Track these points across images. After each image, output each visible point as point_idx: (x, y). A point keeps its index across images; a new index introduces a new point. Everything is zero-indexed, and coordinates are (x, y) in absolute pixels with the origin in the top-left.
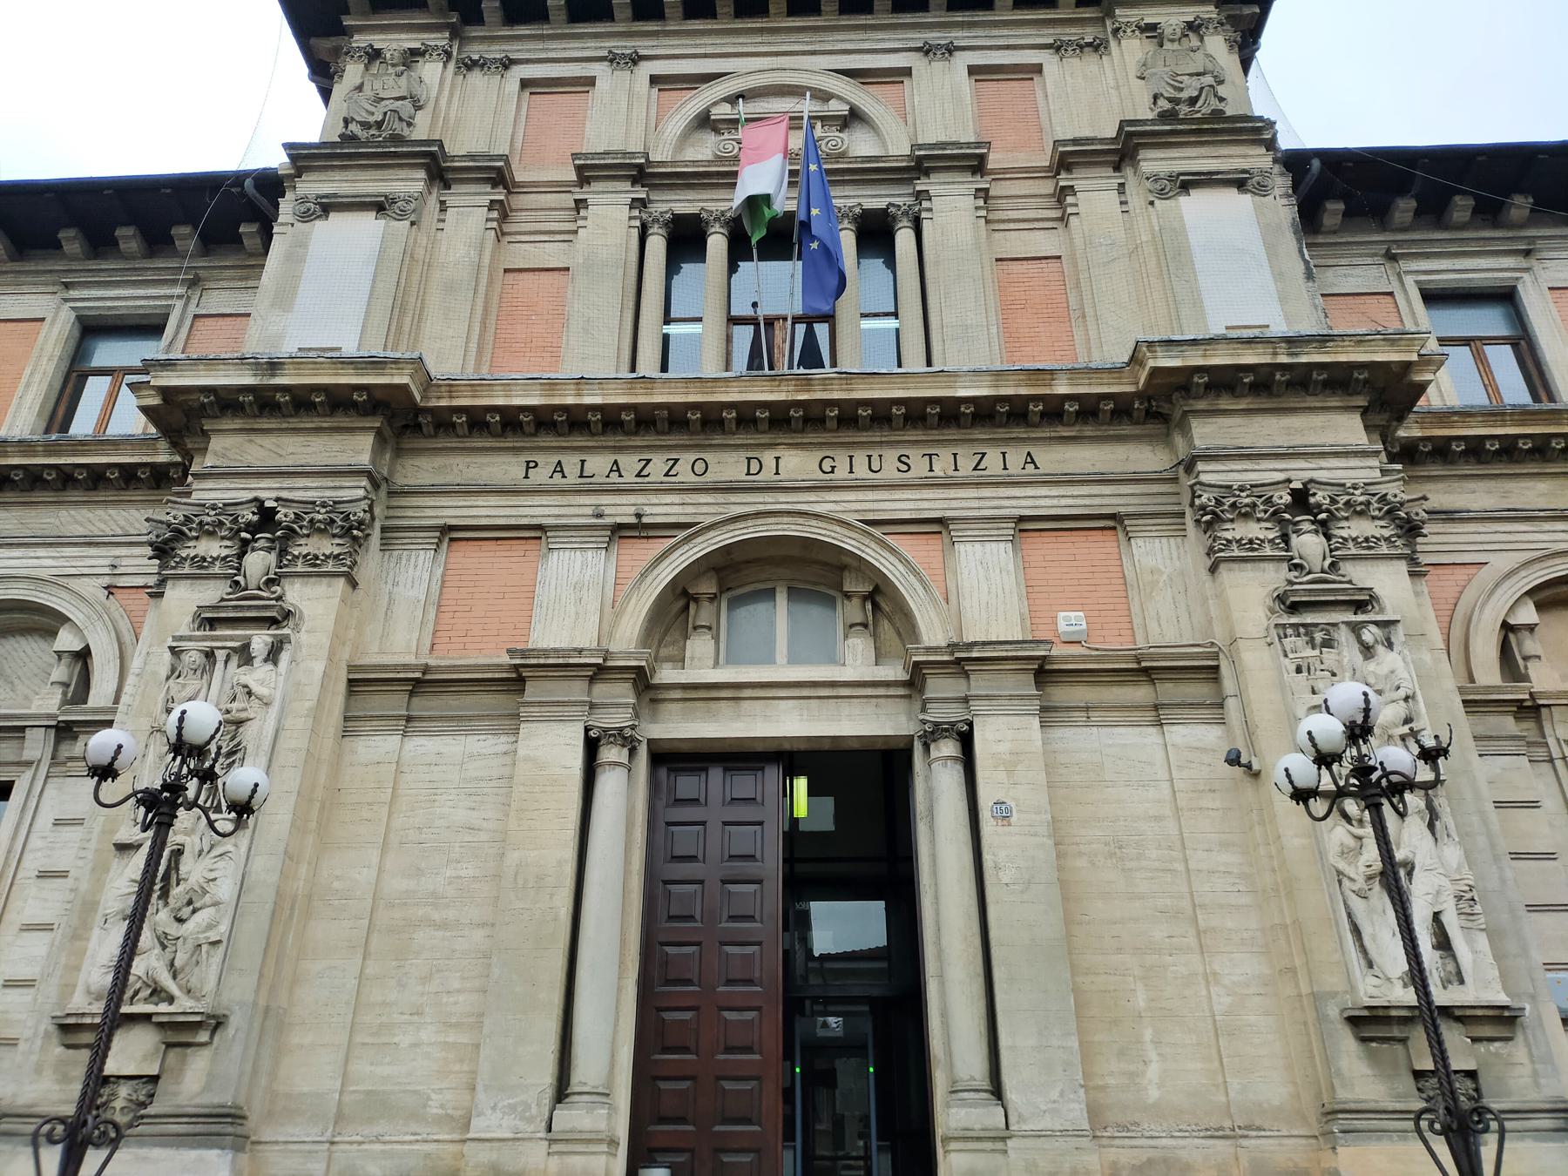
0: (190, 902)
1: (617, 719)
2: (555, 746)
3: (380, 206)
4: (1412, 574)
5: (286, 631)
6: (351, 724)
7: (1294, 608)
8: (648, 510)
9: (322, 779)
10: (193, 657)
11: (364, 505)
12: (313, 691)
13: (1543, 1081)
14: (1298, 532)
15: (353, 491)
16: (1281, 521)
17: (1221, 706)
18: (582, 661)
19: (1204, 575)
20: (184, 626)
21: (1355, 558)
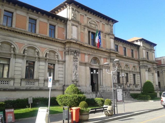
1: (90, 67)
3: (77, 26)
10: (74, 61)
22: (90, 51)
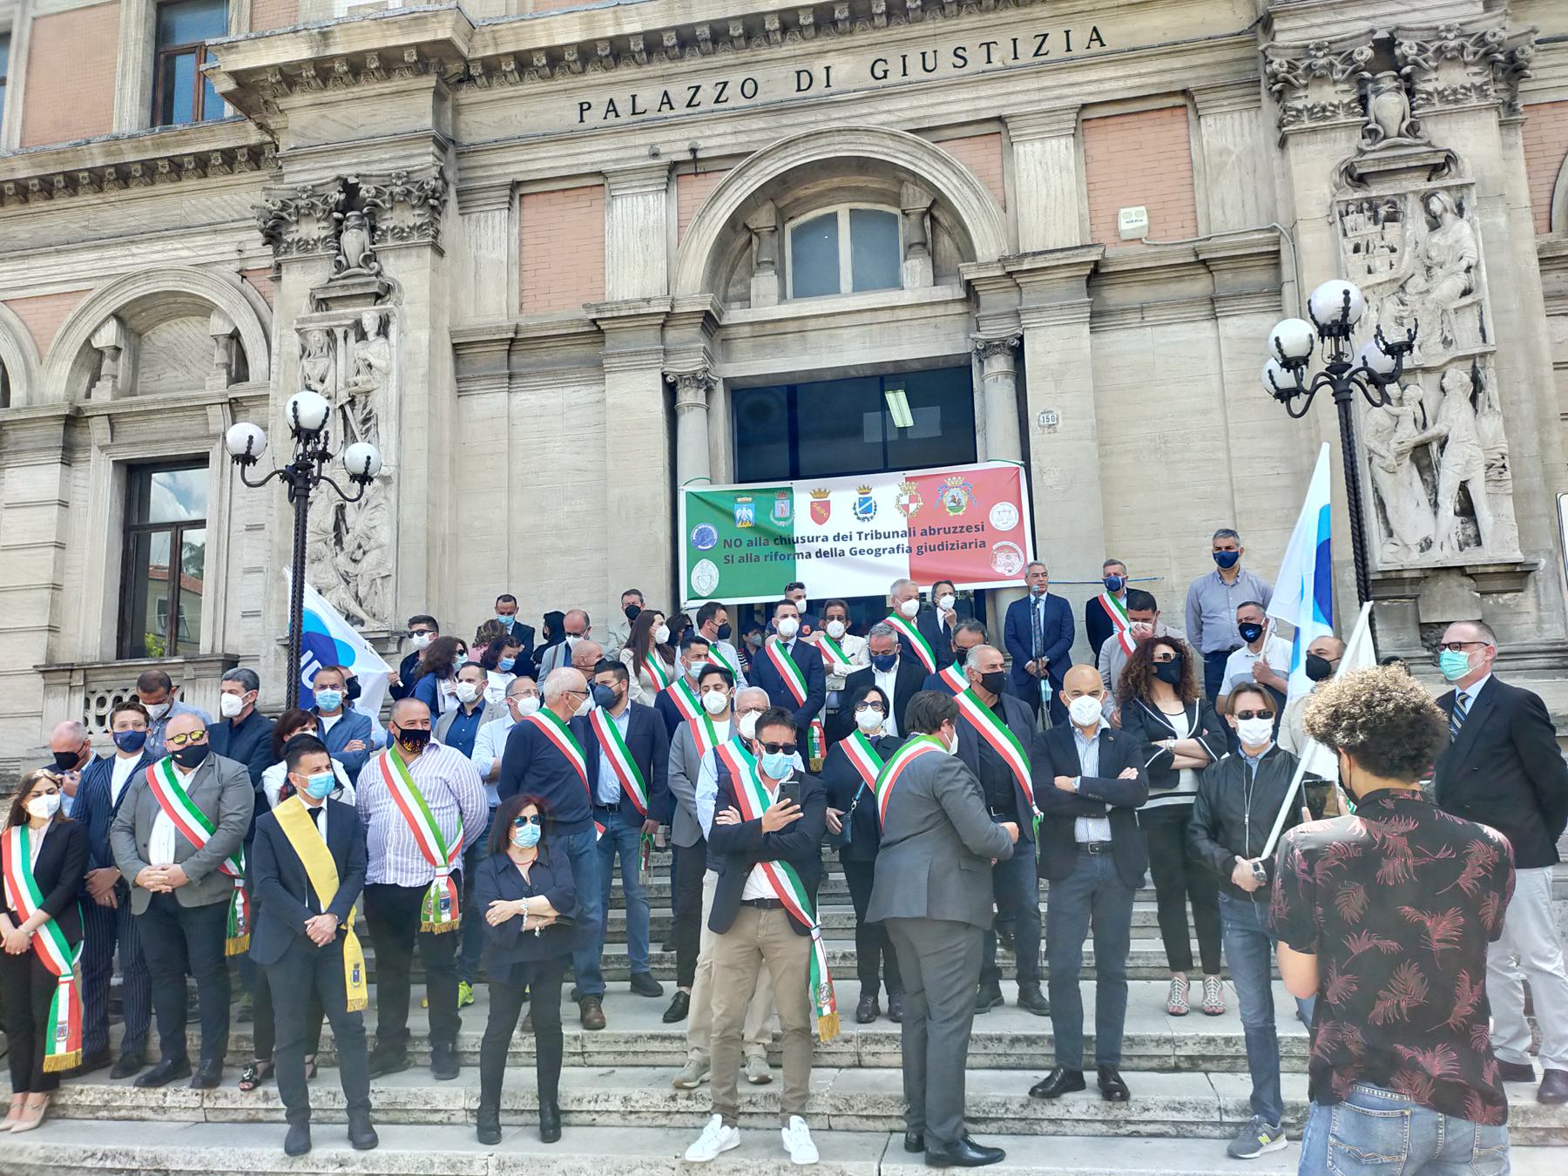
0: (360, 547)
1: (689, 363)
2: (635, 393)
4: (1501, 124)
5: (389, 305)
6: (463, 381)
7: (1361, 180)
8: (701, 144)
9: (447, 435)
10: (317, 338)
11: (434, 172)
12: (423, 357)
13: (1546, 626)
14: (1377, 92)
15: (424, 160)
16: (1362, 82)
17: (1279, 293)
18: (652, 310)
19: (1275, 152)
20: (304, 307)
21: (1438, 114)
22: (708, 93)
